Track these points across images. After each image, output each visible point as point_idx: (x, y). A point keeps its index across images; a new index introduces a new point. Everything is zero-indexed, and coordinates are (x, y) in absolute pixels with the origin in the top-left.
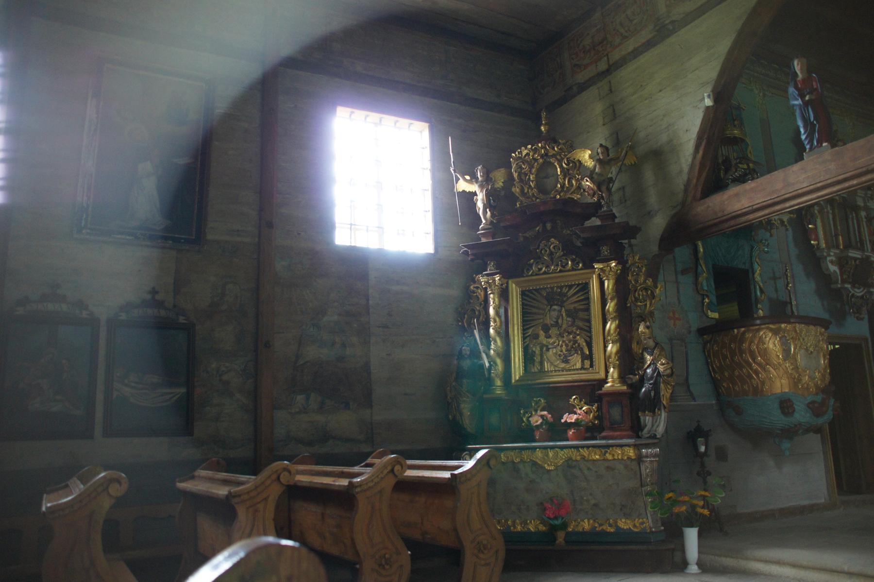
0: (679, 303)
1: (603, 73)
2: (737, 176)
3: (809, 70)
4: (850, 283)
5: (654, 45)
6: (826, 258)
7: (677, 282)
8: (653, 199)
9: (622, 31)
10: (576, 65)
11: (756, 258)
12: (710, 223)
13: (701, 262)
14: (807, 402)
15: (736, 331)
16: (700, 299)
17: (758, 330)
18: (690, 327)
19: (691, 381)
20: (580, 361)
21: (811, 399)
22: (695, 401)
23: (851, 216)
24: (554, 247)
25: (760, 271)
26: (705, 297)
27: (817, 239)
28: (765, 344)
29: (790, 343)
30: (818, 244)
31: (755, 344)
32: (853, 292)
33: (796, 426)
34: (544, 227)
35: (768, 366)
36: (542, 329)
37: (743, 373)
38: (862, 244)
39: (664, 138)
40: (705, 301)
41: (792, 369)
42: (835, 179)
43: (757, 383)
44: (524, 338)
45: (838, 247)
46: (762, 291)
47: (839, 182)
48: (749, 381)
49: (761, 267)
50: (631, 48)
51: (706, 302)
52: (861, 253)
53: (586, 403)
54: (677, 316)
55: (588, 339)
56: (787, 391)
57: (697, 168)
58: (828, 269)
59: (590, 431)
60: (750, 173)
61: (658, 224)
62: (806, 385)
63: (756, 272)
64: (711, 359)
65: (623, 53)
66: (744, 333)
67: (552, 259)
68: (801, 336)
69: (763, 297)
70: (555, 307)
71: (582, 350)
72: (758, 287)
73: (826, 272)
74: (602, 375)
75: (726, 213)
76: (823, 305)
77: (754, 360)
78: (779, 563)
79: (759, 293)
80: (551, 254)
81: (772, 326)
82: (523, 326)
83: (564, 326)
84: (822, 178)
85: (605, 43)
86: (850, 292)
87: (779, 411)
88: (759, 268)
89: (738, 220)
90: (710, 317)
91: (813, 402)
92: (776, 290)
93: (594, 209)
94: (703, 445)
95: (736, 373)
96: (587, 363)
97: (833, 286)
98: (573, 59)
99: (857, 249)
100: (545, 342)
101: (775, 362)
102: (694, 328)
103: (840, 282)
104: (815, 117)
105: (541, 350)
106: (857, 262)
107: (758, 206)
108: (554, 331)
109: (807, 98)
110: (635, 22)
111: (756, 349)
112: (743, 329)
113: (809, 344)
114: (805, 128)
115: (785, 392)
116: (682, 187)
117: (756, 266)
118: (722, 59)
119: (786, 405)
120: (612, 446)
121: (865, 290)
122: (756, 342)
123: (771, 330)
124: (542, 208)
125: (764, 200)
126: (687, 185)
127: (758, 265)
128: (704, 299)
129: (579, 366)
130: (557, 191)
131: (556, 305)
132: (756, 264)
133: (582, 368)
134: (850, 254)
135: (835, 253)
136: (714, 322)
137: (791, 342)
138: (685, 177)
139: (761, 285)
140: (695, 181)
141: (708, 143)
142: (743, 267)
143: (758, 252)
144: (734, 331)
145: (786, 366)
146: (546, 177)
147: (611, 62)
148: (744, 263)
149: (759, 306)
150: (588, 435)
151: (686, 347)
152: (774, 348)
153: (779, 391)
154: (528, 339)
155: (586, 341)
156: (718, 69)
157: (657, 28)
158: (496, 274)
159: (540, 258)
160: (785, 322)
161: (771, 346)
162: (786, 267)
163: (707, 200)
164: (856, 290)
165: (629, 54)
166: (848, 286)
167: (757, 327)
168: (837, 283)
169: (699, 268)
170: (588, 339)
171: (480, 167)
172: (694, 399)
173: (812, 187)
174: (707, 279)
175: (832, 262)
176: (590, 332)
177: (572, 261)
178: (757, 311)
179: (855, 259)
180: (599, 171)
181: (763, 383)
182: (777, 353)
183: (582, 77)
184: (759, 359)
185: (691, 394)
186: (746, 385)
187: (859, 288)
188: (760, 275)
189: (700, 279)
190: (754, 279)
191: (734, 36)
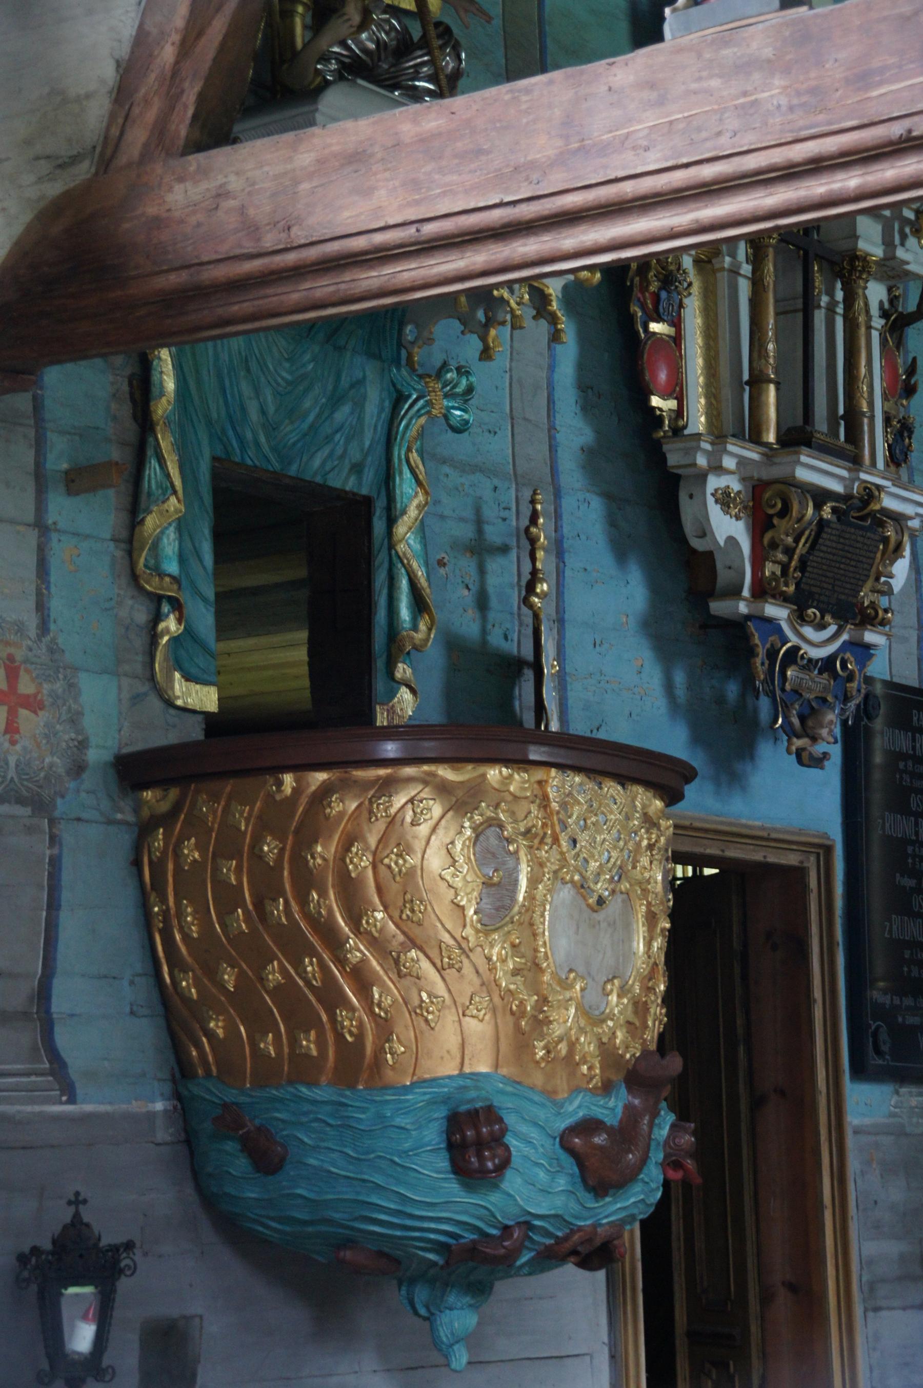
0: (44, 627)
2: (365, 50)
4: (785, 599)
6: (702, 478)
7: (41, 526)
11: (409, 450)
12: (221, 272)
13: (165, 441)
14: (563, 1125)
15: (288, 779)
16: (142, 616)
17: (387, 786)
18: (83, 745)
19: (58, 1005)
21: (581, 1114)
22: (72, 1100)
23: (825, 299)
25: (420, 507)
26: (166, 608)
27: (677, 390)
28: (409, 850)
29: (516, 852)
30: (679, 413)
31: (367, 848)
32: (794, 640)
33: (506, 1230)
35: (413, 953)
37: (302, 974)
38: (854, 436)
40: (162, 626)
41: (516, 972)
42: (777, 157)
43: (361, 1025)
45: (755, 437)
46: (420, 604)
48: (324, 1018)
49: (427, 493)
51: (167, 631)
52: (844, 473)
54: (26, 687)
56: (484, 1068)
58: (705, 531)
60: (424, 44)
62: (563, 1048)
63: (404, 512)
64: (163, 900)
66: (326, 791)
68: (565, 826)
69: (422, 627)
72: (404, 583)
73: (697, 544)
75: (299, 235)
76: (669, 687)
77: (355, 920)
79: (405, 613)
81: (445, 773)
84: (726, 145)
86: (785, 640)
88: (421, 498)
89: (347, 276)
90: (179, 703)
91: (589, 1126)
92: (482, 603)
94: (85, 1318)
95: (274, 976)
97: (718, 607)
99: (828, 450)
101: (446, 938)
102: (97, 755)
103: (746, 593)
106: (827, 512)
107: (447, 226)
111: (370, 873)
113: (594, 865)
115: (475, 1076)
116: (109, 73)
117: (405, 485)
121: (845, 637)
122: (373, 841)
123: (443, 789)
125: (472, 205)
127: (419, 483)
128: (157, 618)
132: (407, 474)
134: (802, 474)
135: (742, 462)
136: (196, 733)
137: (522, 854)
139: (421, 573)
140: (168, 53)
142: (350, 485)
143: (423, 420)
144: (280, 783)
145: (489, 959)
148: (357, 469)
149: (403, 670)
151: (54, 840)
152: (448, 874)
153: (450, 1069)
160: (506, 762)
161: (435, 861)
162: (533, 502)
163: (220, 156)
164: (808, 631)
166: (777, 612)
167: (382, 772)
168: (735, 592)
169: (152, 468)
172: (69, 1092)
173: (678, 178)
174: (183, 526)
175: (725, 499)
178: (392, 693)
179: (821, 496)
181: (385, 1028)
182: (457, 895)
184: (379, 915)
185: (58, 1065)
186: (313, 1034)
187: (822, 627)
188: (422, 528)
189: (151, 522)
190: (391, 546)
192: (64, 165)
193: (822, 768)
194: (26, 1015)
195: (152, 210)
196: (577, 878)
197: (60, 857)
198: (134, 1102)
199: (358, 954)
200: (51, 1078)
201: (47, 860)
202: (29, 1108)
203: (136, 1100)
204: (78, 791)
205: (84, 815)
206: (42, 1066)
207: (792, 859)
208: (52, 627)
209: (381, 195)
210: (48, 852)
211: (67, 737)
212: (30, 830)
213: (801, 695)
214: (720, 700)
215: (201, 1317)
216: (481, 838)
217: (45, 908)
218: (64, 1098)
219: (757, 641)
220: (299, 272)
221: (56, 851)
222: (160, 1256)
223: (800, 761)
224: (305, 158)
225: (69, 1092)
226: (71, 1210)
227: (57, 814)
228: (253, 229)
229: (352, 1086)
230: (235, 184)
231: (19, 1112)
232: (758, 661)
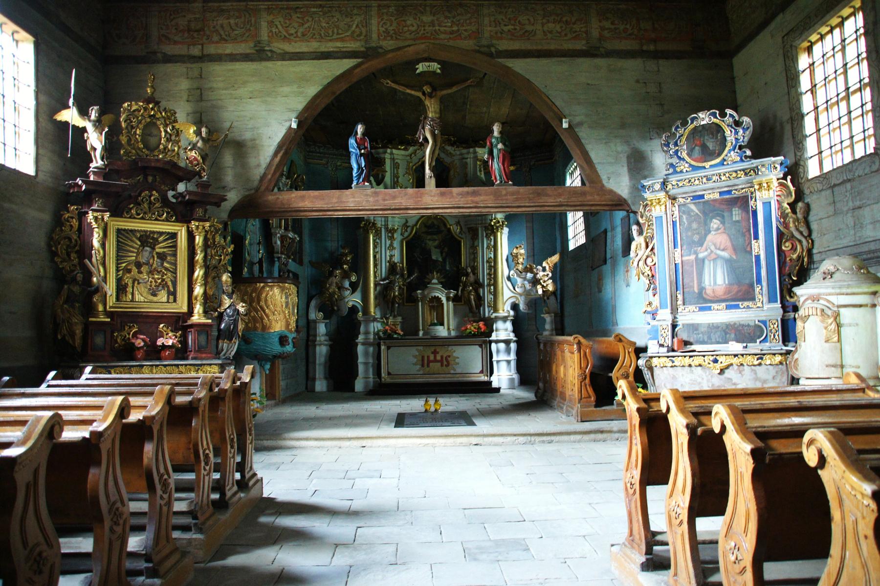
1: (194, 57)
3: (364, 134)
5: (252, 60)
8: (229, 177)
9: (222, 33)
10: (163, 35)
12: (277, 210)
20: (166, 296)
24: (154, 199)
34: (146, 178)
36: (136, 266)
39: (248, 136)
42: (371, 208)
44: (118, 270)
47: (372, 210)
50: (228, 51)
53: (172, 331)
55: (173, 279)
57: (274, 168)
59: (181, 352)
61: (233, 197)
65: (220, 51)
66: (263, 287)
67: (150, 208)
70: (148, 249)
71: (168, 287)
74: (185, 309)
78: (307, 439)
80: (150, 203)
82: (117, 260)
83: (155, 266)
85: (201, 33)
87: (278, 343)
93: (188, 175)
96: (171, 297)
98: (162, 29)
100: (137, 277)
104: (365, 166)
105: (133, 283)
108: (144, 269)
109: (363, 151)
110: (236, 32)
112: (262, 285)
114: (358, 169)
116: (259, 178)
118: (309, 99)
119: (283, 340)
120: (204, 365)
124: (153, 164)
126: (263, 178)
129: (165, 299)
130: (160, 151)
131: (149, 247)
133: (168, 302)
138: (261, 170)
140: (269, 176)
141: (286, 153)
146: (149, 135)
147: (205, 53)
150: (180, 355)
154: (121, 272)
155: (171, 280)
156: (304, 104)
157: (257, 48)
158: (106, 211)
159: (140, 204)
165: (227, 55)
170: (173, 279)
171: (96, 108)
176: (176, 273)
177: (168, 213)
180: (202, 147)
183: (170, 49)
191: (320, 88)
192: (249, 190)
195: (265, 199)
209: (306, 203)
220: (290, 211)
224: (293, 195)
228: (283, 204)
230: (280, 197)
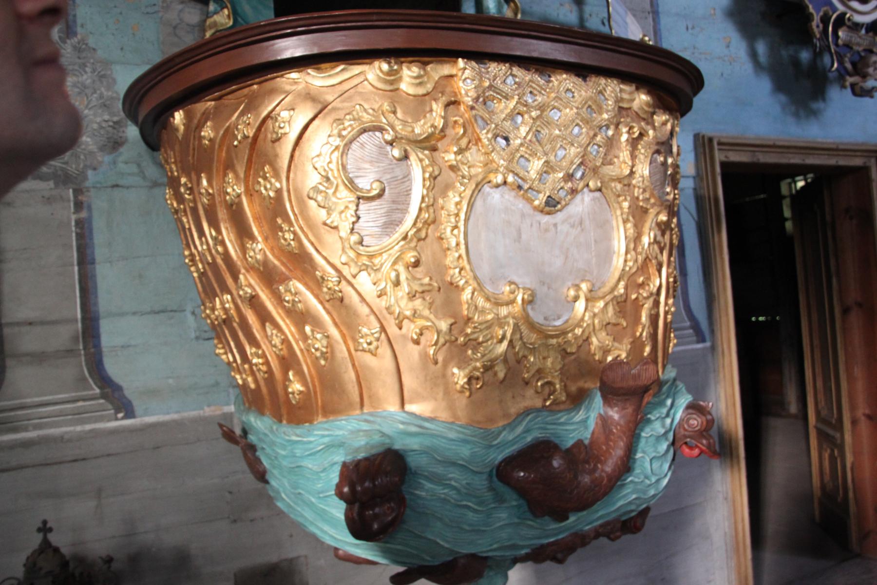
21: (529, 439)
22: (130, 413)
32: (841, 8)
76: (753, 55)
86: (835, 9)
151: (79, 206)
172: (127, 409)
193: (872, 97)
194: (70, 352)
196: (510, 178)
197: (89, 220)
198: (206, 408)
199: (249, 291)
200: (102, 401)
201: (73, 223)
202: (79, 428)
203: (209, 406)
204: (115, 163)
205: (121, 182)
206: (91, 392)
207: (857, 162)
208: (79, 30)
210: (73, 217)
211: (98, 120)
212: (49, 200)
213: (851, 48)
214: (796, 63)
215: (306, 557)
216: (354, 146)
217: (75, 262)
218: (120, 415)
219: (811, 9)
221: (84, 214)
222: (252, 521)
223: (855, 93)
225: (127, 409)
226: (40, 536)
227: (88, 184)
229: (280, 421)
231: (66, 433)
232: (814, 24)
